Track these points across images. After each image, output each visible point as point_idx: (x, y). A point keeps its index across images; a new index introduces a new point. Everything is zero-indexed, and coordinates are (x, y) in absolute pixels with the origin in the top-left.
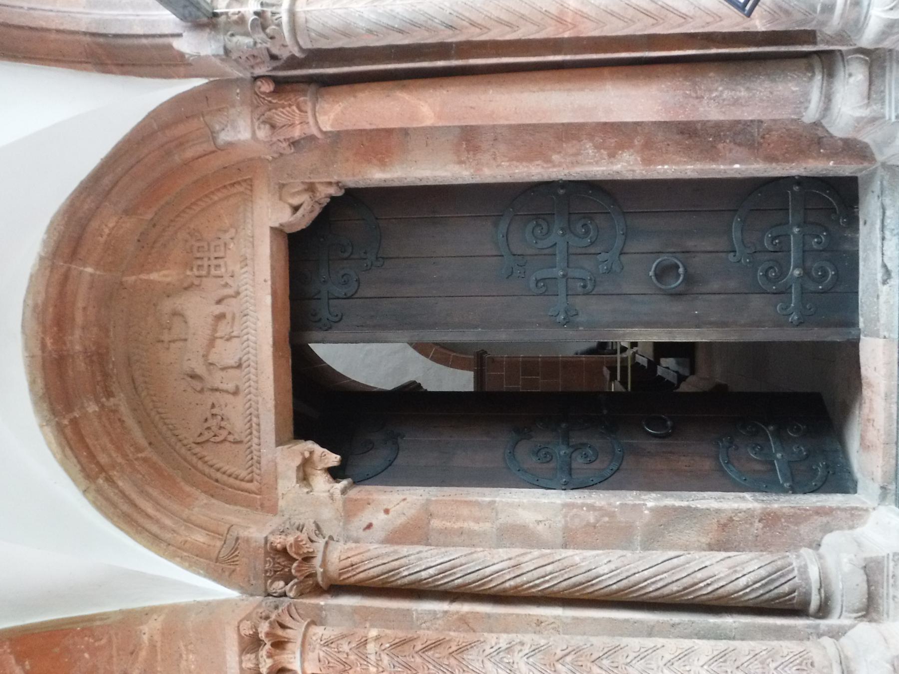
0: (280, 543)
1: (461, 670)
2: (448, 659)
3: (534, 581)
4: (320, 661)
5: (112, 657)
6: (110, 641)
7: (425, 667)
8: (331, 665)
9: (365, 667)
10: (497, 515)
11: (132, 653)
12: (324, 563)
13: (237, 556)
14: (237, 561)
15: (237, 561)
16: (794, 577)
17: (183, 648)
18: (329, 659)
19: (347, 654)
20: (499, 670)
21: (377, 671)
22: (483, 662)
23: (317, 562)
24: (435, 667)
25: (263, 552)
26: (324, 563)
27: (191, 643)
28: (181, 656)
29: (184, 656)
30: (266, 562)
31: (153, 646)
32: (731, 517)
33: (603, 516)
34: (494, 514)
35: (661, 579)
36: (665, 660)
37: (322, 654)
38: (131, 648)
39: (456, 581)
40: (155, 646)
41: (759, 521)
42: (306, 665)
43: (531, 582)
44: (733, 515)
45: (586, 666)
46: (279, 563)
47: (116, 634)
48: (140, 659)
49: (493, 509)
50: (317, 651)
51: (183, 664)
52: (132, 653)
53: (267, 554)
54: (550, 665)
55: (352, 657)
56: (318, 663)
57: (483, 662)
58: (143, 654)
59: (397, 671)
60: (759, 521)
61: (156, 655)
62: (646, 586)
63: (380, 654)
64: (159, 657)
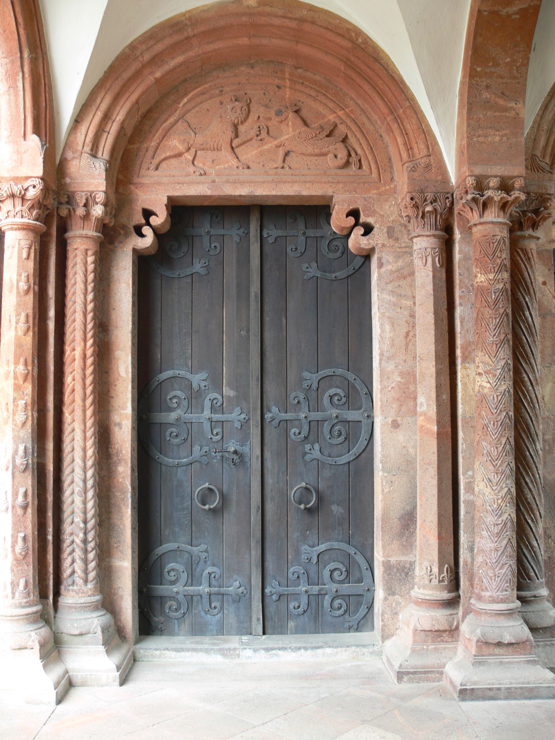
0: (551, 205)
1: (497, 342)
2: (504, 333)
3: (529, 395)
4: (493, 236)
5: (502, 78)
6: (515, 78)
7: (497, 316)
8: (491, 245)
9: (493, 270)
10: (547, 367)
11: (503, 93)
12: (531, 237)
13: (538, 171)
14: (534, 171)
15: (534, 171)
16: (538, 579)
17: (504, 132)
18: (497, 243)
19: (501, 257)
20: (500, 370)
21: (490, 280)
22: (504, 358)
23: (530, 232)
24: (498, 323)
25: (544, 192)
26: (531, 237)
27: (508, 139)
28: (498, 130)
29: (498, 133)
30: (536, 194)
31: (507, 110)
32: (551, 537)
33: (549, 445)
34: (547, 365)
35: (534, 486)
36: (510, 488)
37: (499, 238)
38: (507, 93)
39: (524, 337)
40: (506, 111)
41: (549, 557)
42: (491, 226)
43: (528, 393)
44: (553, 538)
45: (505, 434)
46: (532, 203)
47: (519, 83)
48: (497, 99)
49: (551, 364)
50: (500, 234)
51: (492, 132)
52: (503, 93)
53: (541, 195)
54: (505, 407)
55: (499, 261)
56: (492, 235)
57: (504, 358)
58: (501, 102)
59: (491, 294)
60: (549, 557)
61: (499, 112)
62: (529, 476)
63: (502, 282)
64: (497, 114)
